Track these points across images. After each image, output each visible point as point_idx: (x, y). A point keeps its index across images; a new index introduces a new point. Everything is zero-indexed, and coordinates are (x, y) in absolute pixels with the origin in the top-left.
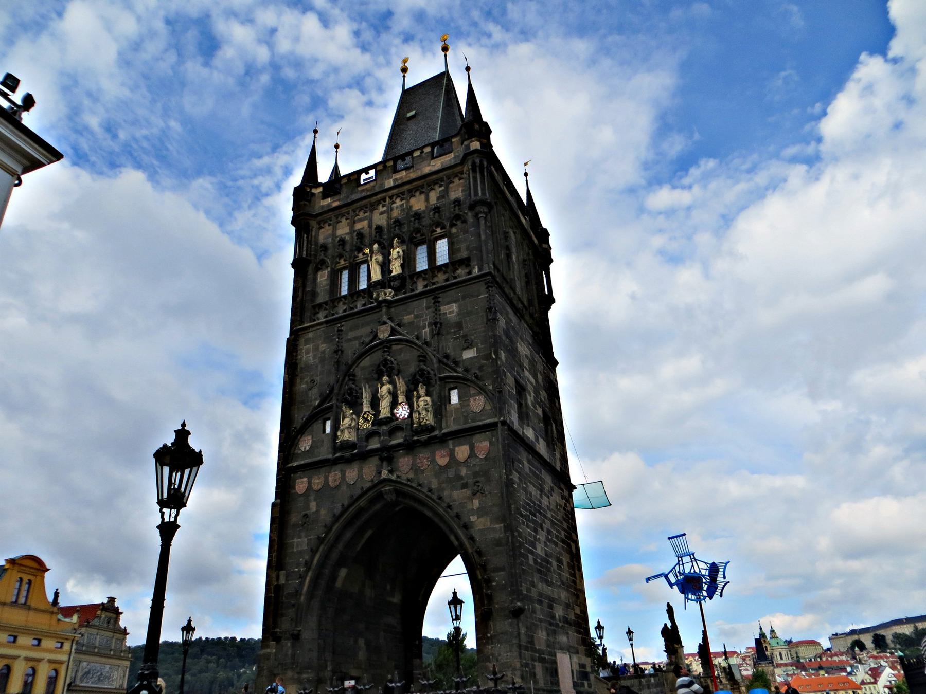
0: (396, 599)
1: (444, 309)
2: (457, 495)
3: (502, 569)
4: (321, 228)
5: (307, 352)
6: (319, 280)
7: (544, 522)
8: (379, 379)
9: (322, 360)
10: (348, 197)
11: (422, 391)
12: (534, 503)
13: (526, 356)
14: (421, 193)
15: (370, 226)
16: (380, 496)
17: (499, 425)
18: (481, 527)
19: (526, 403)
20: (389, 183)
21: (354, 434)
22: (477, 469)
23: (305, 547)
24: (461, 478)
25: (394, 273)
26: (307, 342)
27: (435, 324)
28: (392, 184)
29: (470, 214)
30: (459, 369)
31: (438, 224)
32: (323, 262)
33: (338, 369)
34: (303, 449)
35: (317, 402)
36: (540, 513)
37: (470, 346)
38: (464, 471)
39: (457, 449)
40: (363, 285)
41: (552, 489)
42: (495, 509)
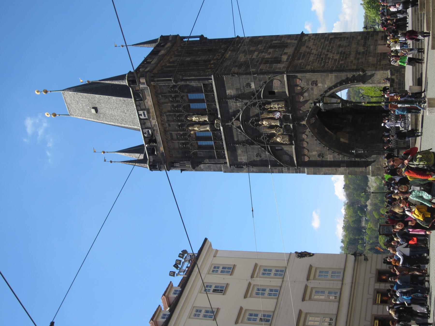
0: (350, 117)
3: (347, 75)
6: (202, 156)
7: (324, 53)
11: (267, 106)
12: (317, 58)
13: (245, 56)
19: (270, 58)
23: (332, 156)
25: (207, 119)
27: (236, 100)
30: (260, 90)
31: (182, 98)
33: (252, 144)
34: (288, 159)
36: (321, 55)
37: (249, 85)
39: (296, 92)
41: (307, 47)
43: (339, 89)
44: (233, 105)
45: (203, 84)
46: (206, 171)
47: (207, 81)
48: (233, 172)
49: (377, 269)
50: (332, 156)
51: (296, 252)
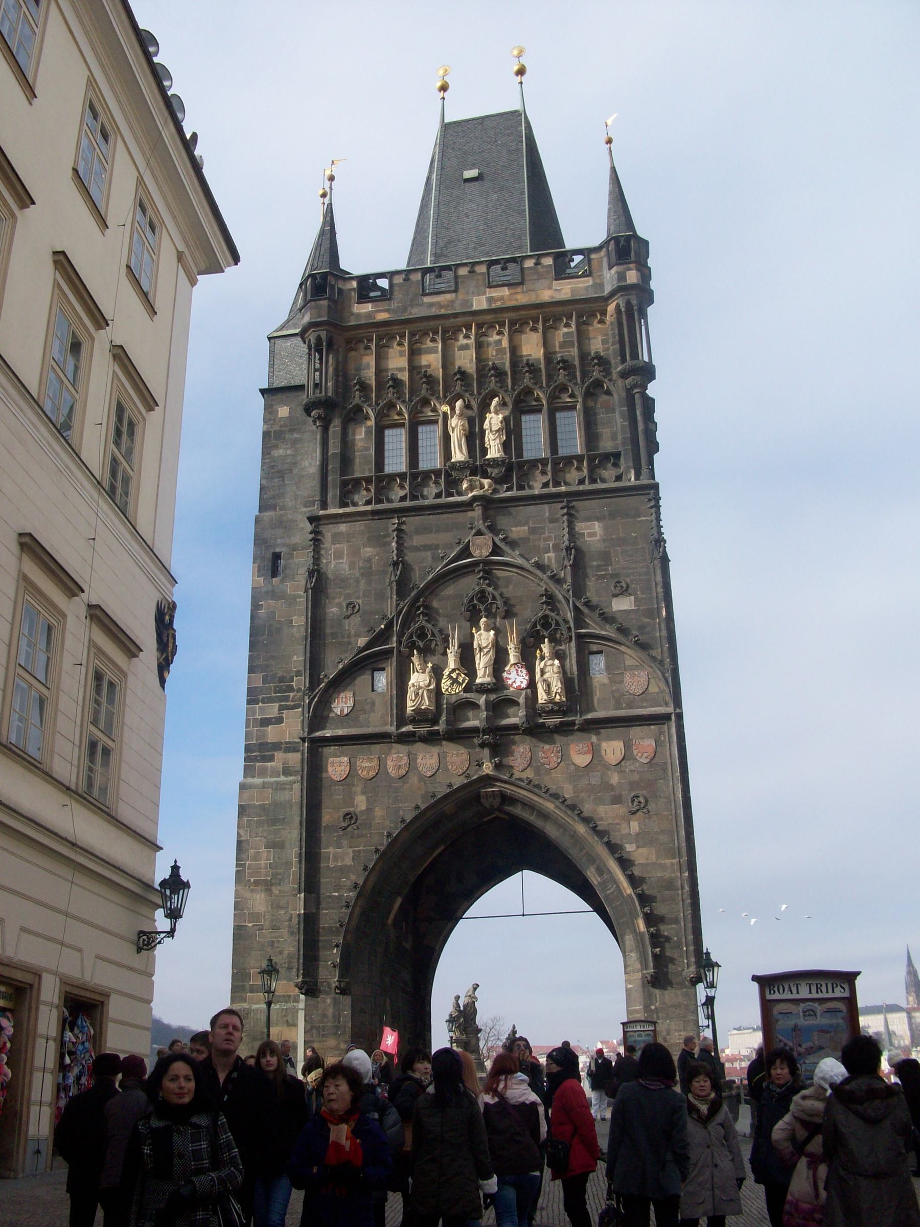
0: (408, 945)
1: (580, 526)
2: (606, 813)
4: (352, 349)
5: (339, 555)
8: (474, 622)
9: (367, 573)
10: (405, 309)
14: (534, 329)
15: (444, 367)
16: (478, 797)
17: (673, 717)
18: (641, 862)
20: (479, 303)
21: (434, 700)
22: (636, 777)
23: (348, 861)
24: (612, 788)
26: (337, 538)
27: (568, 549)
28: (484, 306)
29: (620, 382)
31: (564, 388)
32: (358, 409)
33: (401, 595)
34: (338, 711)
35: (362, 642)
38: (615, 779)
39: (604, 745)
40: (431, 459)
42: (663, 838)
43: (619, 889)
44: (549, 538)
45: (617, 455)
46: (263, 464)
47: (631, 464)
48: (255, 544)
49: (108, 996)
50: (348, 861)
51: (173, 607)
